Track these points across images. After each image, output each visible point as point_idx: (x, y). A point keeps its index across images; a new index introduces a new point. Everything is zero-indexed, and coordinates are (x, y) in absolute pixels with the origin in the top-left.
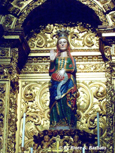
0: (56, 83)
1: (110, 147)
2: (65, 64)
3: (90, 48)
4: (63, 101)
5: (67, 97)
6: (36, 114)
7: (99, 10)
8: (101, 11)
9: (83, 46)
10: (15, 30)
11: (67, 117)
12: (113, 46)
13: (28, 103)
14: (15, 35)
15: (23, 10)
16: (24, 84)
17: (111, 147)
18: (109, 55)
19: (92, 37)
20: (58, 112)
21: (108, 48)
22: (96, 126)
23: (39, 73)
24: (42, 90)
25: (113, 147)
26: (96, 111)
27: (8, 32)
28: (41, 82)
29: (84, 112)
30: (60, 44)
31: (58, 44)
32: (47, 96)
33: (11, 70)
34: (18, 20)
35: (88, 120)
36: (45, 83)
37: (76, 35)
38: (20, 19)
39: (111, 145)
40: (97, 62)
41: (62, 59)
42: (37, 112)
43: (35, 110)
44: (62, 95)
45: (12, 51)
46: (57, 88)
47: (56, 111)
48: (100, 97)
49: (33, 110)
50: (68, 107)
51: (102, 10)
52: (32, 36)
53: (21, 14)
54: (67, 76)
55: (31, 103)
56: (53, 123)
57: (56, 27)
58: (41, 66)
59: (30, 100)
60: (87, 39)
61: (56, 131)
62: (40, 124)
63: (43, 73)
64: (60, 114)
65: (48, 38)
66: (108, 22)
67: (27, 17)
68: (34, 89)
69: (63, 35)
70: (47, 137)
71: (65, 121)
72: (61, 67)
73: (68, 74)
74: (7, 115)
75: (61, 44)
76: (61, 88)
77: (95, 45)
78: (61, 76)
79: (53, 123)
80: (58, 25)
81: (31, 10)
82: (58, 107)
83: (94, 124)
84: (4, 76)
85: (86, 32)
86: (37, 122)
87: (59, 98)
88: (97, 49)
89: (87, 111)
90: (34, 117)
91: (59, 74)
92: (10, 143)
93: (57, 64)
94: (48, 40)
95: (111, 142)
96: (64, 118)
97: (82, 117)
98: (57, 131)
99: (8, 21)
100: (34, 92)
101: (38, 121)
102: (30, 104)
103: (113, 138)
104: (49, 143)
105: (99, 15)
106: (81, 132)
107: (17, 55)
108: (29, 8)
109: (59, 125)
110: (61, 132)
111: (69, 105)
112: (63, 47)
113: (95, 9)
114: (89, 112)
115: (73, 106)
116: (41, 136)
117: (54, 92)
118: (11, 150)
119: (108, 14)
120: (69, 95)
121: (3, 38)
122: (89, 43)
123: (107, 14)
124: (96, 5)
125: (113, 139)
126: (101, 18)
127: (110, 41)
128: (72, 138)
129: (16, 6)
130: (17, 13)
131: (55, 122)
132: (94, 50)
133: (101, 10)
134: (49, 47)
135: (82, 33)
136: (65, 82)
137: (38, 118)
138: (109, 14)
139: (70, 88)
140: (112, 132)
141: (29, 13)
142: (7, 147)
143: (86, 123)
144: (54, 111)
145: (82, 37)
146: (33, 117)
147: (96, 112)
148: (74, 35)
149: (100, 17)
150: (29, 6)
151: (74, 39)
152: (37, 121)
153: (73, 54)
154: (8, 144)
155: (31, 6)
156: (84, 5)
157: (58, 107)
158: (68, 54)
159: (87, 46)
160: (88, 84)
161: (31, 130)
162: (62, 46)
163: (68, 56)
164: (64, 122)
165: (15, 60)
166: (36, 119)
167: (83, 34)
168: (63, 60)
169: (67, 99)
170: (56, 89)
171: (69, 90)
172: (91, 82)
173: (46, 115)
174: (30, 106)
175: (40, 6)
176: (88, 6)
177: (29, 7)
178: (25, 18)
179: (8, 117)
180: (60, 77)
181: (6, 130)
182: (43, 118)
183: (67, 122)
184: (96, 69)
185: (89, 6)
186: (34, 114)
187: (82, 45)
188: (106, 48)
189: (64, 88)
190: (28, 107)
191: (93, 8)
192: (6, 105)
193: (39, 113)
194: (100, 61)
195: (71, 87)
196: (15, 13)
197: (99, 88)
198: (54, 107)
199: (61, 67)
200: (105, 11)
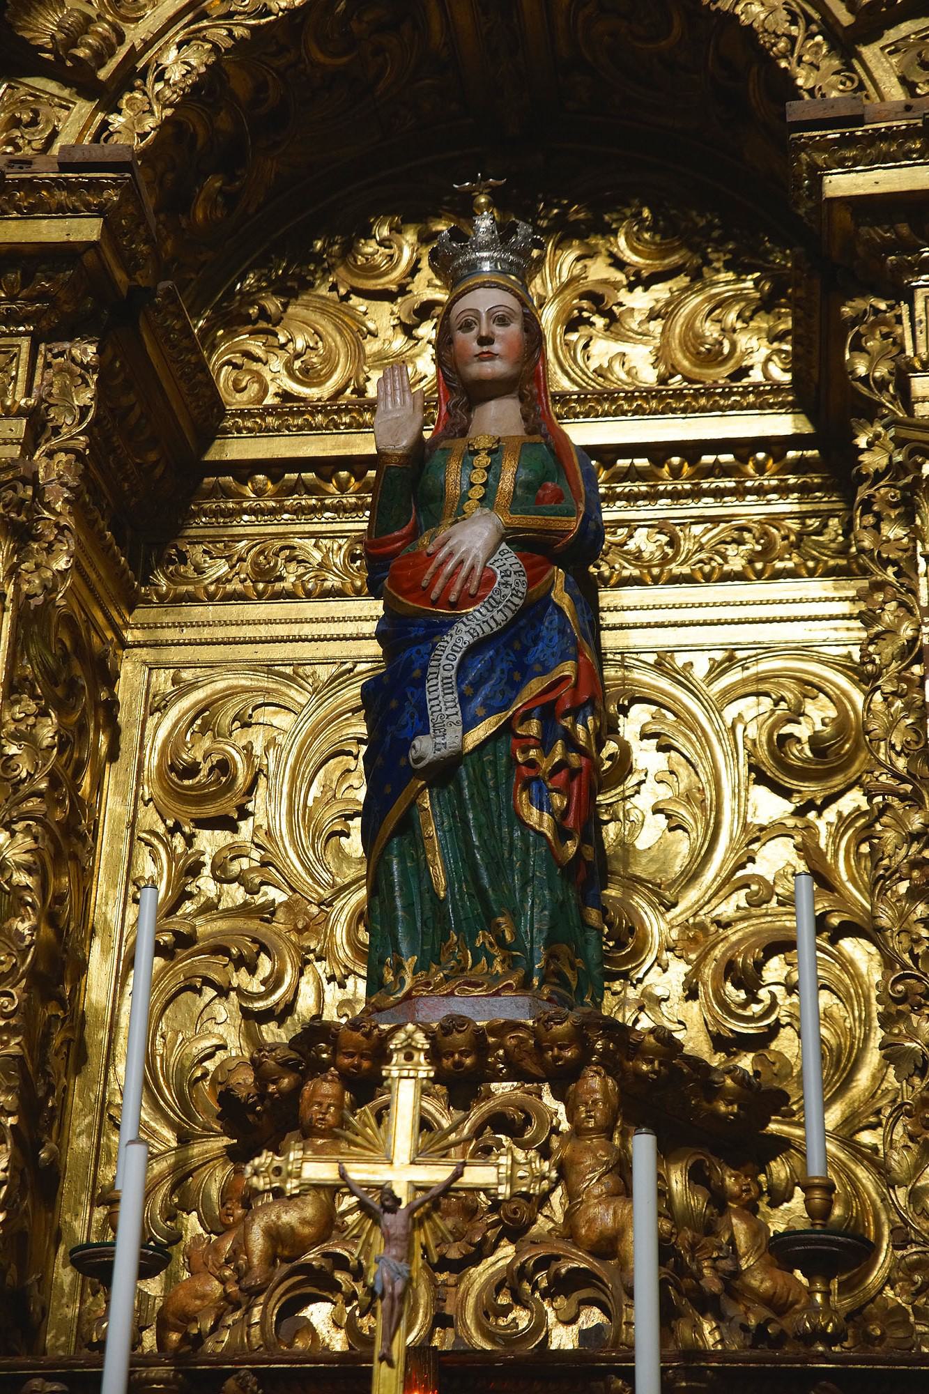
0: (421, 632)
4: (479, 780)
6: (254, 924)
7: (794, 22)
8: (814, 28)
11: (515, 915)
12: (920, 295)
13: (189, 840)
14: (62, 211)
15: (148, 45)
19: (731, 317)
20: (438, 873)
21: (877, 311)
23: (290, 595)
24: (315, 733)
26: (771, 891)
29: (668, 910)
30: (459, 335)
31: (451, 342)
35: (708, 972)
38: (117, 121)
42: (267, 912)
43: (252, 891)
44: (468, 726)
45: (48, 365)
46: (424, 669)
47: (422, 871)
48: (803, 774)
49: (236, 895)
50: (524, 837)
51: (816, 16)
52: (248, 320)
53: (129, 76)
54: (516, 567)
56: (389, 978)
59: (210, 810)
60: (689, 325)
62: (290, 1008)
64: (449, 885)
65: (374, 335)
69: (487, 267)
70: (327, 1088)
71: (495, 951)
75: (474, 333)
76: (462, 668)
78: (467, 564)
81: (216, 48)
82: (432, 830)
83: (756, 1009)
85: (683, 280)
86: (263, 989)
87: (444, 752)
90: (234, 951)
91: (451, 554)
94: (371, 347)
96: (488, 922)
97: (655, 941)
100: (248, 750)
101: (273, 982)
102: (210, 842)
105: (794, 60)
107: (85, 397)
108: (205, 28)
109: (437, 986)
110: (458, 1037)
111: (533, 816)
112: (491, 356)
113: (762, 16)
114: (714, 902)
115: (571, 821)
117: (401, 708)
119: (868, 41)
120: (534, 728)
126: (810, 85)
128: (558, 1096)
130: (101, 57)
131: (410, 963)
132: (751, 398)
133: (809, 20)
135: (647, 283)
138: (882, 43)
139: (546, 671)
141: (203, 69)
143: (691, 994)
144: (403, 872)
146: (224, 951)
148: (582, 296)
151: (584, 330)
152: (264, 982)
155: (220, 17)
157: (432, 830)
161: (210, 1065)
162: (476, 348)
164: (490, 964)
166: (252, 970)
167: (661, 291)
170: (421, 682)
171: (535, 686)
172: (731, 659)
173: (340, 934)
174: (207, 859)
177: (205, 23)
178: (165, 107)
180: (454, 573)
182: (319, 959)
184: (767, 553)
186: (240, 923)
188: (858, 319)
189: (491, 669)
190: (194, 870)
193: (280, 915)
196: (82, 53)
200: (845, 18)
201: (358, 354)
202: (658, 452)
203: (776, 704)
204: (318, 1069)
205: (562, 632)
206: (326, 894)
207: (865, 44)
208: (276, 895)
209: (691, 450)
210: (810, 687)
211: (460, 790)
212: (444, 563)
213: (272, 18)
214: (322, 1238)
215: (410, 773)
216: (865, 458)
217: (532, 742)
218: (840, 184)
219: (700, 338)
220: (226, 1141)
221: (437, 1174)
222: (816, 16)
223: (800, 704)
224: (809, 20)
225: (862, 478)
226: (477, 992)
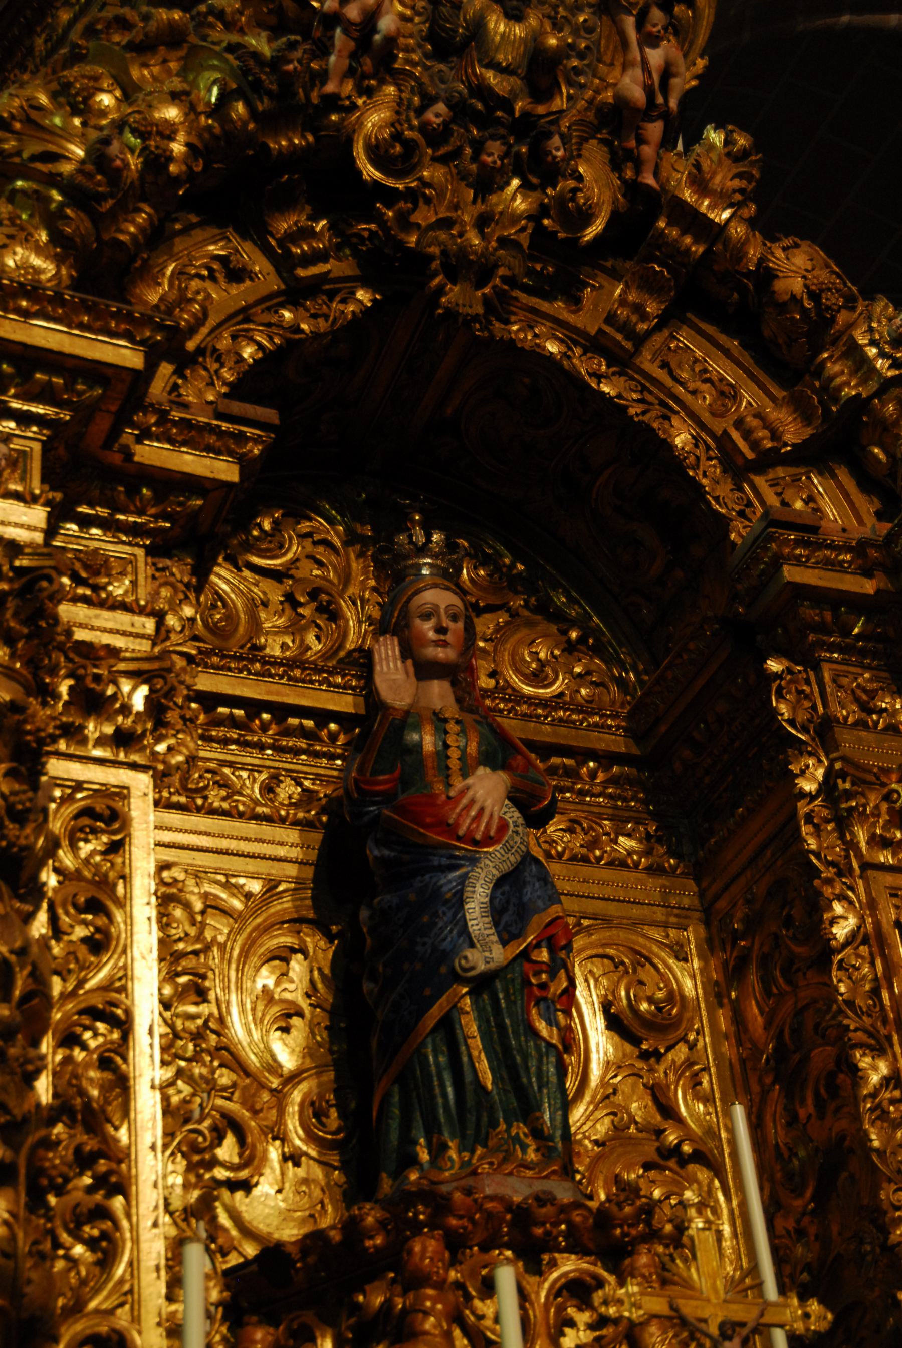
0: (445, 861)
5: (527, 966)
18: (802, 717)
41: (446, 721)
50: (537, 1047)
56: (424, 1156)
71: (529, 1141)
72: (454, 763)
79: (424, 1156)
82: (473, 1029)
87: (492, 965)
91: (472, 801)
98: (509, 1207)
105: (700, 473)
110: (547, 1210)
112: (445, 644)
116: (368, 1243)
120: (544, 955)
123: (752, 477)
133: (708, 448)
136: (512, 859)
139: (538, 911)
147: (632, 1130)
169: (527, 982)
170: (459, 901)
176: (627, 407)
183: (547, 1152)
188: (778, 676)
191: (655, 425)
198: (434, 1030)
203: (616, 967)
204: (416, 1228)
206: (275, 1083)
217: (544, 967)
224: (708, 448)
226: (529, 1173)
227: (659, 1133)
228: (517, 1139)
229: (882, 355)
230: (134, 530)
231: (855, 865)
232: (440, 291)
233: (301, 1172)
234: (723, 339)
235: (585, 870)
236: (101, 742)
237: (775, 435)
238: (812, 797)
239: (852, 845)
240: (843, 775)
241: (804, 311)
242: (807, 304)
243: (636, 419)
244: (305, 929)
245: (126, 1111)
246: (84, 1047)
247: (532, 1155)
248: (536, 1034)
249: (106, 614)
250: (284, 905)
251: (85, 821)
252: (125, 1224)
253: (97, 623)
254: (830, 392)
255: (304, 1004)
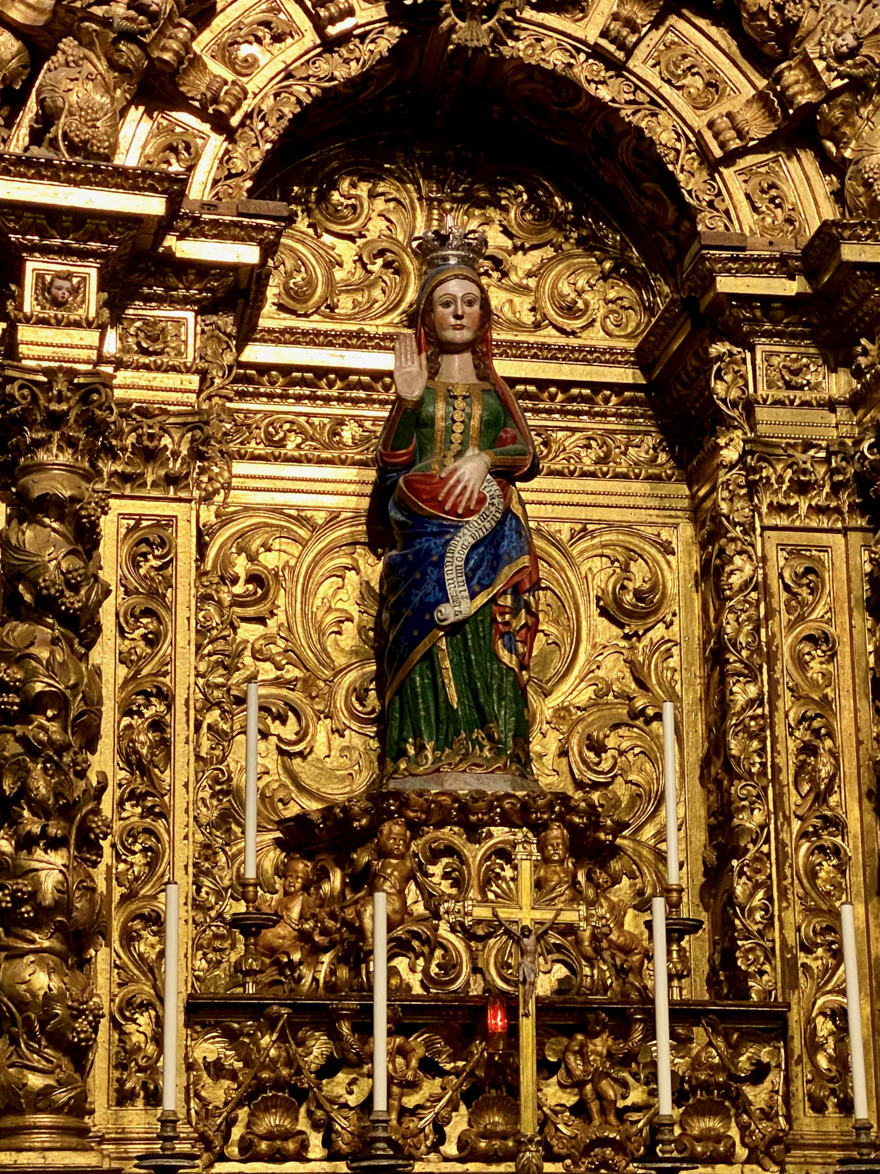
0: (435, 529)
1: (752, 895)
2: (475, 423)
3: (573, 341)
4: (476, 633)
5: (495, 608)
6: (284, 692)
7: (678, 140)
8: (691, 147)
9: (537, 326)
10: (240, 215)
12: (759, 349)
16: (213, 520)
17: (760, 894)
18: (734, 394)
19: (581, 283)
21: (731, 354)
22: (615, 776)
23: (297, 460)
24: (315, 562)
25: (770, 899)
26: (609, 688)
27: (196, 221)
28: (309, 514)
29: (546, 696)
30: (440, 309)
31: (432, 311)
32: (342, 594)
33: (206, 441)
34: (227, 151)
35: (574, 741)
36: (334, 519)
37: (497, 263)
39: (757, 886)
40: (613, 424)
41: (455, 397)
42: (289, 684)
43: (279, 668)
44: (473, 596)
45: (203, 332)
46: (442, 557)
47: (437, 688)
48: (631, 615)
49: (267, 671)
50: (500, 670)
51: (693, 139)
54: (498, 493)
55: (258, 629)
56: (412, 751)
57: (380, 204)
58: (302, 420)
59: (250, 612)
60: (554, 286)
61: (446, 800)
63: (321, 462)
65: (341, 265)
66: (727, 212)
67: (280, 136)
68: (269, 550)
70: (397, 829)
71: (485, 742)
72: (457, 437)
73: (499, 484)
74: (187, 701)
75: (451, 309)
77: (598, 324)
79: (412, 751)
80: (395, 194)
81: (299, 102)
82: (447, 664)
84: (162, 473)
85: (549, 252)
86: (293, 737)
87: (460, 617)
88: (624, 352)
89: (565, 687)
90: (274, 710)
91: (458, 481)
92: (207, 859)
93: (430, 422)
94: (339, 274)
95: (758, 871)
98: (456, 799)
99: (174, 150)
101: (302, 736)
102: (248, 632)
103: (765, 849)
104: (409, 864)
105: (678, 167)
106: (575, 810)
108: (289, 86)
109: (456, 765)
110: (481, 804)
111: (505, 656)
112: (462, 327)
114: (575, 693)
116: (356, 824)
117: (423, 580)
118: (212, 899)
119: (727, 167)
120: (508, 601)
121: (169, 253)
122: (570, 310)
123: (722, 169)
124: (664, 109)
125: (768, 855)
126: (689, 188)
127: (746, 319)
129: (216, 68)
132: (607, 356)
133: (688, 141)
134: (350, 318)
135: (525, 251)
136: (488, 525)
137: (299, 720)
138: (735, 168)
139: (511, 561)
140: (758, 817)
141: (290, 116)
142: (191, 880)
143: (564, 753)
144: (423, 685)
145: (529, 275)
147: (610, 697)
149: (681, 177)
150: (289, 76)
152: (297, 734)
153: (504, 367)
154: (195, 865)
155: (301, 79)
156: (597, 102)
158: (484, 371)
159: (556, 327)
160: (565, 536)
162: (453, 321)
163: (482, 377)
164: (481, 750)
165: (217, 381)
166: (284, 722)
167: (536, 256)
168: (460, 404)
169: (494, 620)
170: (440, 565)
171: (507, 573)
172: (584, 529)
173: (340, 702)
175: (350, 82)
176: (619, 110)
177: (291, 82)
178: (266, 142)
179: (192, 713)
180: (461, 494)
181: (186, 785)
182: (326, 718)
185: (626, 112)
186: (274, 691)
187: (528, 318)
188: (720, 358)
191: (643, 125)
192: (181, 642)
194: (632, 416)
195: (514, 554)
197: (626, 569)
198: (421, 660)
199: (457, 437)
200: (718, 153)
201: (330, 280)
202: (542, 384)
203: (613, 563)
204: (390, 816)
205: (519, 533)
206: (328, 673)
207: (726, 167)
208: (292, 672)
209: (565, 386)
210: (633, 554)
211: (465, 640)
212: (455, 486)
213: (336, 82)
214: (402, 922)
215: (433, 625)
216: (724, 452)
217: (507, 610)
218: (726, 284)
219: (561, 295)
220: (279, 834)
221: (548, 915)
222: (693, 139)
223: (628, 565)
224: (688, 141)
225: (721, 465)
226: (479, 770)
227: (631, 699)
228: (475, 742)
229: (829, 69)
230: (185, 301)
231: (757, 525)
232: (452, 29)
233: (344, 742)
234: (713, 31)
235: (591, 484)
236: (154, 484)
237: (741, 135)
238: (732, 466)
239: (756, 509)
240: (752, 453)
241: (770, 21)
242: (773, 14)
243: (627, 120)
244: (359, 549)
245: (168, 759)
246: (141, 715)
247: (487, 753)
248: (499, 660)
249: (160, 375)
250: (343, 532)
251: (144, 548)
252: (166, 837)
253: (155, 384)
254: (786, 100)
255: (354, 611)
